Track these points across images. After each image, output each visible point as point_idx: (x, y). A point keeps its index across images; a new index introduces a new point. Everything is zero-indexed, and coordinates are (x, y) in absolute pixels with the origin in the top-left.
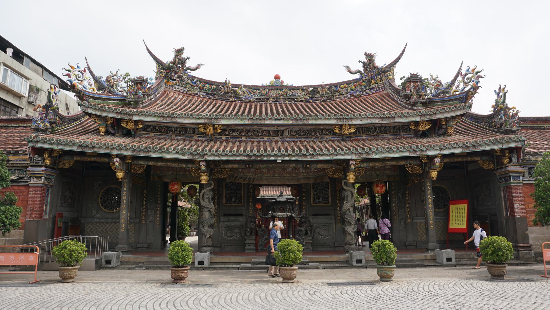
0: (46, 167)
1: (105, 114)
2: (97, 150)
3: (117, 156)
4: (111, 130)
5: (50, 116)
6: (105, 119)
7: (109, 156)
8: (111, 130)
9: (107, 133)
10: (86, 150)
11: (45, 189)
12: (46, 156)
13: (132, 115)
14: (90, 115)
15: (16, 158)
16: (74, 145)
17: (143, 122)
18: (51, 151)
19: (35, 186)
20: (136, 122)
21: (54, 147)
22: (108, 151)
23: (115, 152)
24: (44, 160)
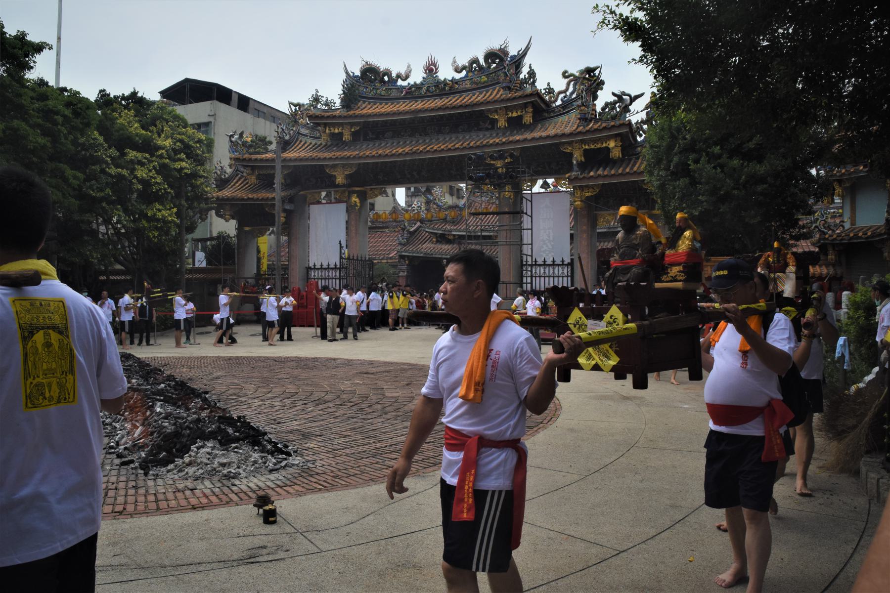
0: (407, 265)
1: (436, 231)
2: (434, 256)
3: (445, 259)
4: (439, 239)
5: (405, 235)
6: (436, 234)
7: (442, 259)
8: (439, 239)
9: (437, 241)
10: (428, 256)
11: (407, 277)
12: (406, 259)
13: (451, 231)
14: (427, 232)
15: (391, 261)
16: (421, 253)
17: (458, 235)
18: (408, 256)
19: (402, 277)
20: (454, 235)
21: (411, 254)
22: (440, 256)
23: (444, 256)
24: (405, 261)
